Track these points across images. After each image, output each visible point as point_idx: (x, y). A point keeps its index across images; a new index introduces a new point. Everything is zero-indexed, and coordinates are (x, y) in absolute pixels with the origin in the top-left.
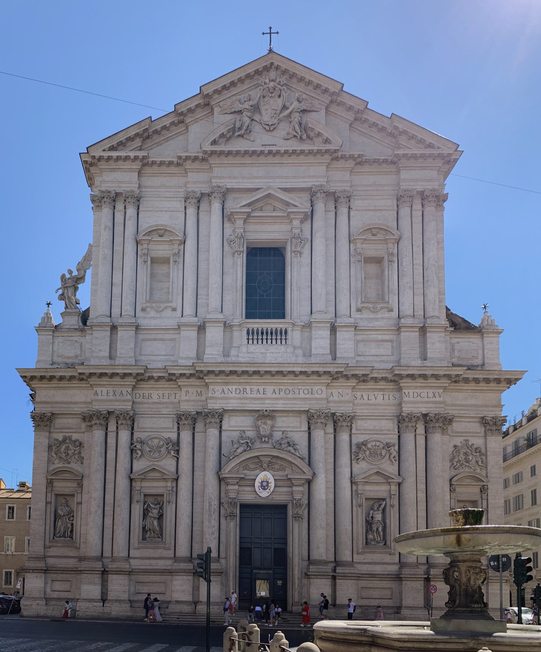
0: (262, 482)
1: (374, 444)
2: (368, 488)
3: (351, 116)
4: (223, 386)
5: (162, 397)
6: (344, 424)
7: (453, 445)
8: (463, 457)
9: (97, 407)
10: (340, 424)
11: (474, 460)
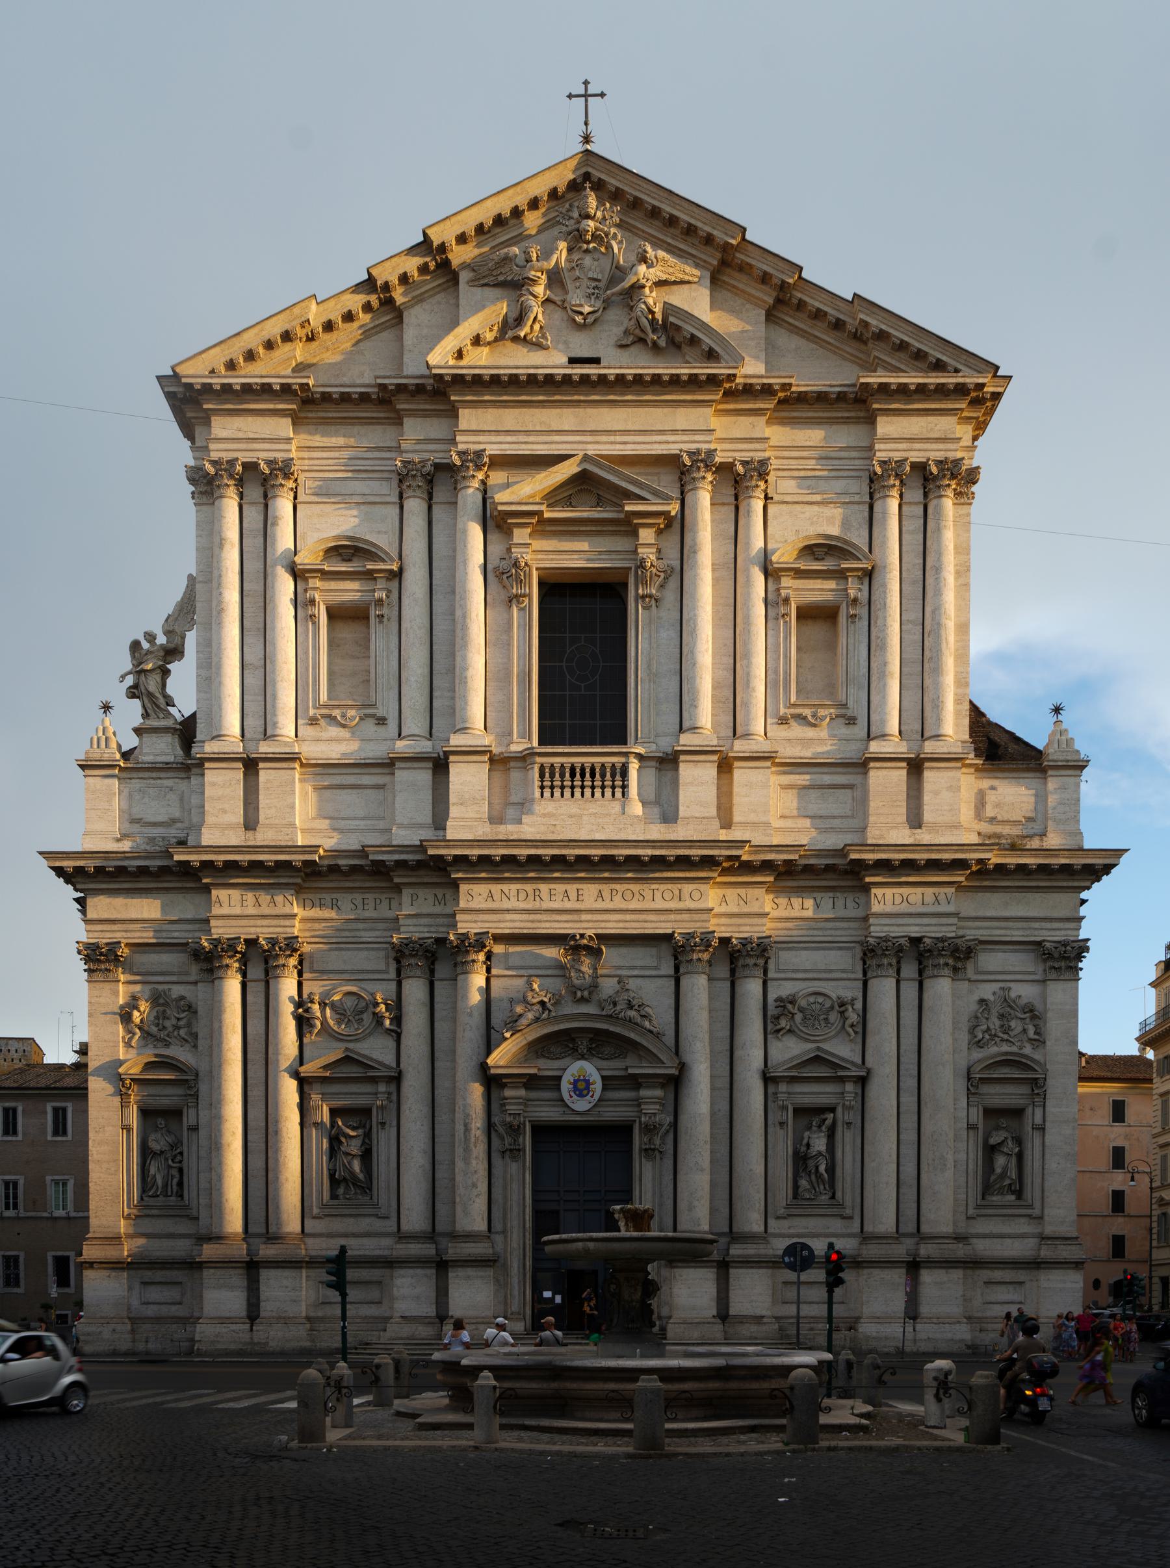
0: (575, 1083)
4: (490, 886)
5: (360, 906)
6: (751, 961)
7: (976, 998)
8: (998, 1023)
9: (221, 931)
10: (741, 962)
11: (1020, 1029)
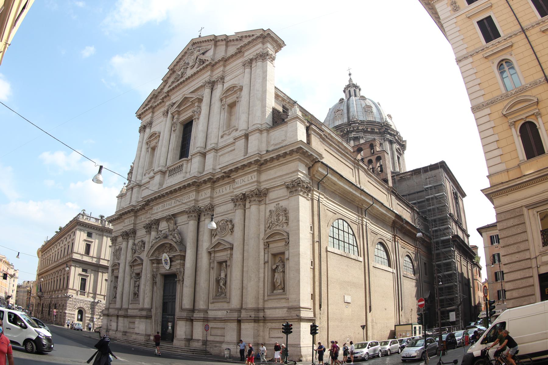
1: (222, 222)
2: (218, 254)
3: (224, 43)
8: (275, 218)
